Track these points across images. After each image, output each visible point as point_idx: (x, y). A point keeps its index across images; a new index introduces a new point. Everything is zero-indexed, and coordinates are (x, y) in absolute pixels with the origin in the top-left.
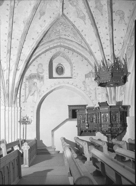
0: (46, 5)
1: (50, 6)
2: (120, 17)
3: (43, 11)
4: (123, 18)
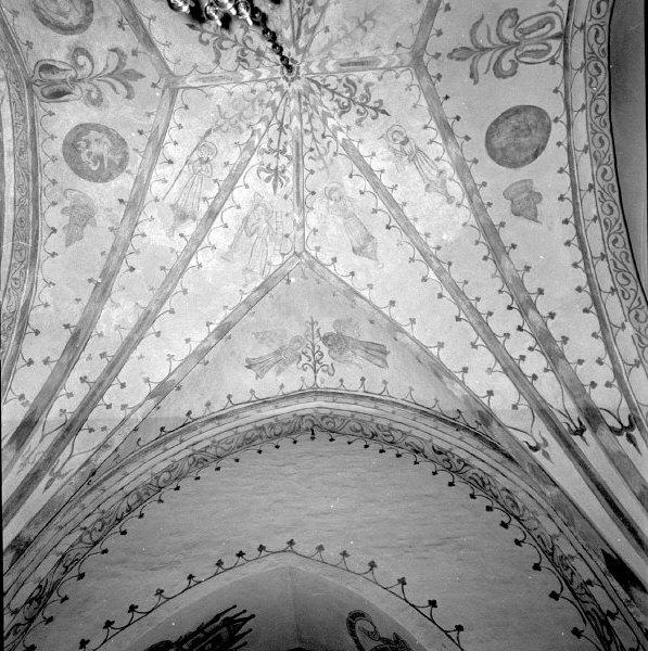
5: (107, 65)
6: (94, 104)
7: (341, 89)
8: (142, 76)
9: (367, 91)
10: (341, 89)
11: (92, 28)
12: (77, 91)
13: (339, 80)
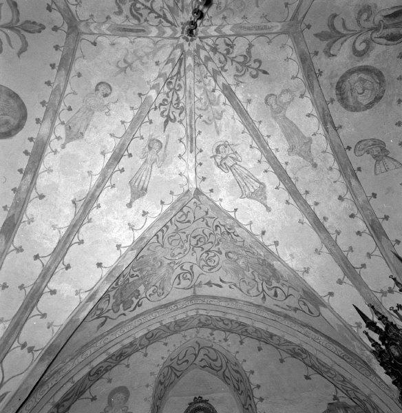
0: (149, 166)
1: (162, 172)
2: (375, 157)
3: (141, 184)
4: (386, 156)
5: (342, 44)
6: (369, 6)
7: (145, 12)
8: (316, 35)
9: (119, 7)
10: (145, 12)
11: (344, 71)
12: (378, 18)
13: (146, 20)
